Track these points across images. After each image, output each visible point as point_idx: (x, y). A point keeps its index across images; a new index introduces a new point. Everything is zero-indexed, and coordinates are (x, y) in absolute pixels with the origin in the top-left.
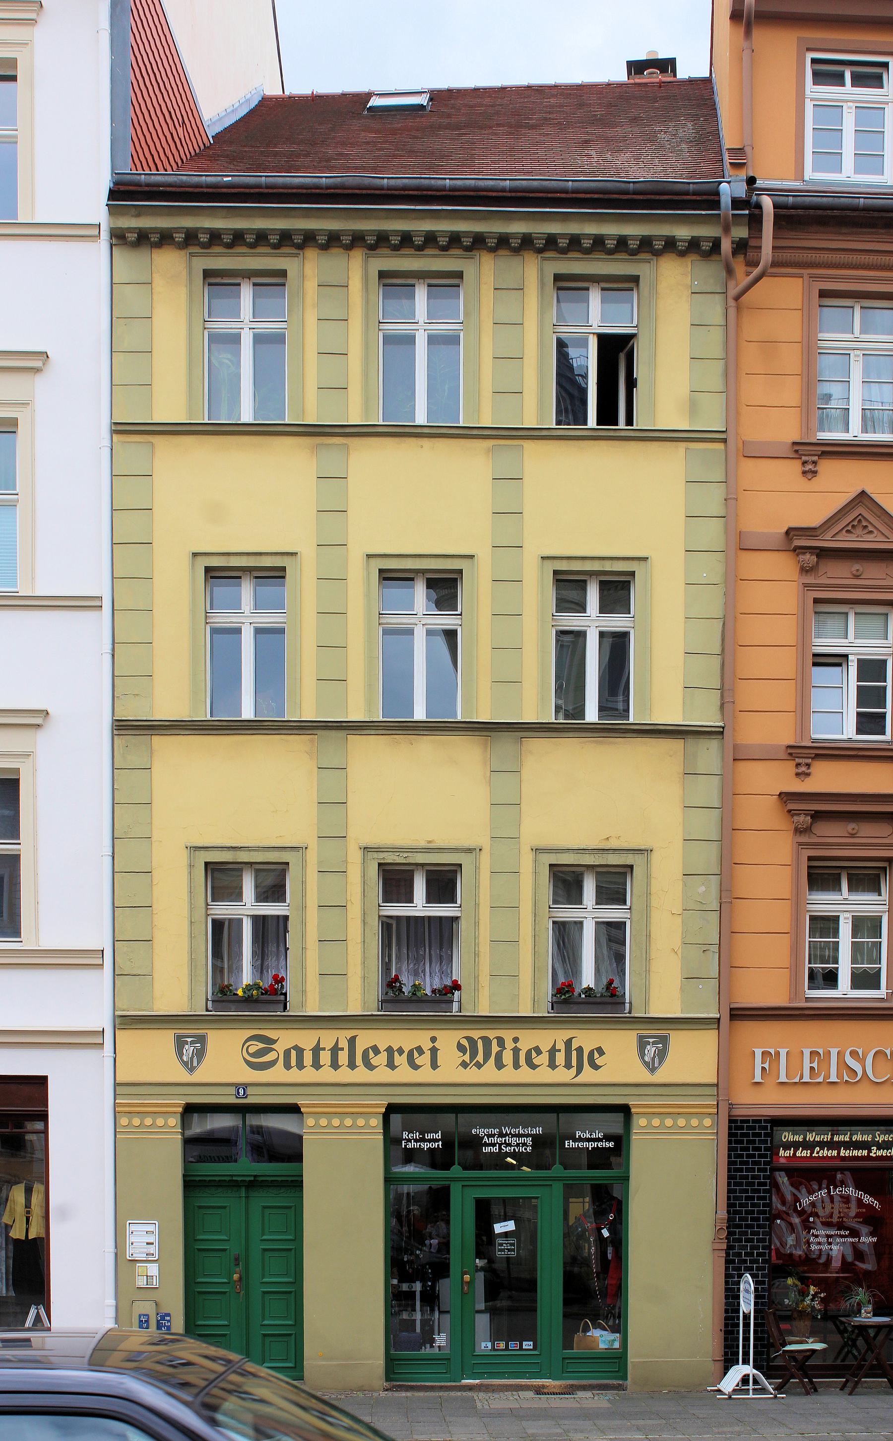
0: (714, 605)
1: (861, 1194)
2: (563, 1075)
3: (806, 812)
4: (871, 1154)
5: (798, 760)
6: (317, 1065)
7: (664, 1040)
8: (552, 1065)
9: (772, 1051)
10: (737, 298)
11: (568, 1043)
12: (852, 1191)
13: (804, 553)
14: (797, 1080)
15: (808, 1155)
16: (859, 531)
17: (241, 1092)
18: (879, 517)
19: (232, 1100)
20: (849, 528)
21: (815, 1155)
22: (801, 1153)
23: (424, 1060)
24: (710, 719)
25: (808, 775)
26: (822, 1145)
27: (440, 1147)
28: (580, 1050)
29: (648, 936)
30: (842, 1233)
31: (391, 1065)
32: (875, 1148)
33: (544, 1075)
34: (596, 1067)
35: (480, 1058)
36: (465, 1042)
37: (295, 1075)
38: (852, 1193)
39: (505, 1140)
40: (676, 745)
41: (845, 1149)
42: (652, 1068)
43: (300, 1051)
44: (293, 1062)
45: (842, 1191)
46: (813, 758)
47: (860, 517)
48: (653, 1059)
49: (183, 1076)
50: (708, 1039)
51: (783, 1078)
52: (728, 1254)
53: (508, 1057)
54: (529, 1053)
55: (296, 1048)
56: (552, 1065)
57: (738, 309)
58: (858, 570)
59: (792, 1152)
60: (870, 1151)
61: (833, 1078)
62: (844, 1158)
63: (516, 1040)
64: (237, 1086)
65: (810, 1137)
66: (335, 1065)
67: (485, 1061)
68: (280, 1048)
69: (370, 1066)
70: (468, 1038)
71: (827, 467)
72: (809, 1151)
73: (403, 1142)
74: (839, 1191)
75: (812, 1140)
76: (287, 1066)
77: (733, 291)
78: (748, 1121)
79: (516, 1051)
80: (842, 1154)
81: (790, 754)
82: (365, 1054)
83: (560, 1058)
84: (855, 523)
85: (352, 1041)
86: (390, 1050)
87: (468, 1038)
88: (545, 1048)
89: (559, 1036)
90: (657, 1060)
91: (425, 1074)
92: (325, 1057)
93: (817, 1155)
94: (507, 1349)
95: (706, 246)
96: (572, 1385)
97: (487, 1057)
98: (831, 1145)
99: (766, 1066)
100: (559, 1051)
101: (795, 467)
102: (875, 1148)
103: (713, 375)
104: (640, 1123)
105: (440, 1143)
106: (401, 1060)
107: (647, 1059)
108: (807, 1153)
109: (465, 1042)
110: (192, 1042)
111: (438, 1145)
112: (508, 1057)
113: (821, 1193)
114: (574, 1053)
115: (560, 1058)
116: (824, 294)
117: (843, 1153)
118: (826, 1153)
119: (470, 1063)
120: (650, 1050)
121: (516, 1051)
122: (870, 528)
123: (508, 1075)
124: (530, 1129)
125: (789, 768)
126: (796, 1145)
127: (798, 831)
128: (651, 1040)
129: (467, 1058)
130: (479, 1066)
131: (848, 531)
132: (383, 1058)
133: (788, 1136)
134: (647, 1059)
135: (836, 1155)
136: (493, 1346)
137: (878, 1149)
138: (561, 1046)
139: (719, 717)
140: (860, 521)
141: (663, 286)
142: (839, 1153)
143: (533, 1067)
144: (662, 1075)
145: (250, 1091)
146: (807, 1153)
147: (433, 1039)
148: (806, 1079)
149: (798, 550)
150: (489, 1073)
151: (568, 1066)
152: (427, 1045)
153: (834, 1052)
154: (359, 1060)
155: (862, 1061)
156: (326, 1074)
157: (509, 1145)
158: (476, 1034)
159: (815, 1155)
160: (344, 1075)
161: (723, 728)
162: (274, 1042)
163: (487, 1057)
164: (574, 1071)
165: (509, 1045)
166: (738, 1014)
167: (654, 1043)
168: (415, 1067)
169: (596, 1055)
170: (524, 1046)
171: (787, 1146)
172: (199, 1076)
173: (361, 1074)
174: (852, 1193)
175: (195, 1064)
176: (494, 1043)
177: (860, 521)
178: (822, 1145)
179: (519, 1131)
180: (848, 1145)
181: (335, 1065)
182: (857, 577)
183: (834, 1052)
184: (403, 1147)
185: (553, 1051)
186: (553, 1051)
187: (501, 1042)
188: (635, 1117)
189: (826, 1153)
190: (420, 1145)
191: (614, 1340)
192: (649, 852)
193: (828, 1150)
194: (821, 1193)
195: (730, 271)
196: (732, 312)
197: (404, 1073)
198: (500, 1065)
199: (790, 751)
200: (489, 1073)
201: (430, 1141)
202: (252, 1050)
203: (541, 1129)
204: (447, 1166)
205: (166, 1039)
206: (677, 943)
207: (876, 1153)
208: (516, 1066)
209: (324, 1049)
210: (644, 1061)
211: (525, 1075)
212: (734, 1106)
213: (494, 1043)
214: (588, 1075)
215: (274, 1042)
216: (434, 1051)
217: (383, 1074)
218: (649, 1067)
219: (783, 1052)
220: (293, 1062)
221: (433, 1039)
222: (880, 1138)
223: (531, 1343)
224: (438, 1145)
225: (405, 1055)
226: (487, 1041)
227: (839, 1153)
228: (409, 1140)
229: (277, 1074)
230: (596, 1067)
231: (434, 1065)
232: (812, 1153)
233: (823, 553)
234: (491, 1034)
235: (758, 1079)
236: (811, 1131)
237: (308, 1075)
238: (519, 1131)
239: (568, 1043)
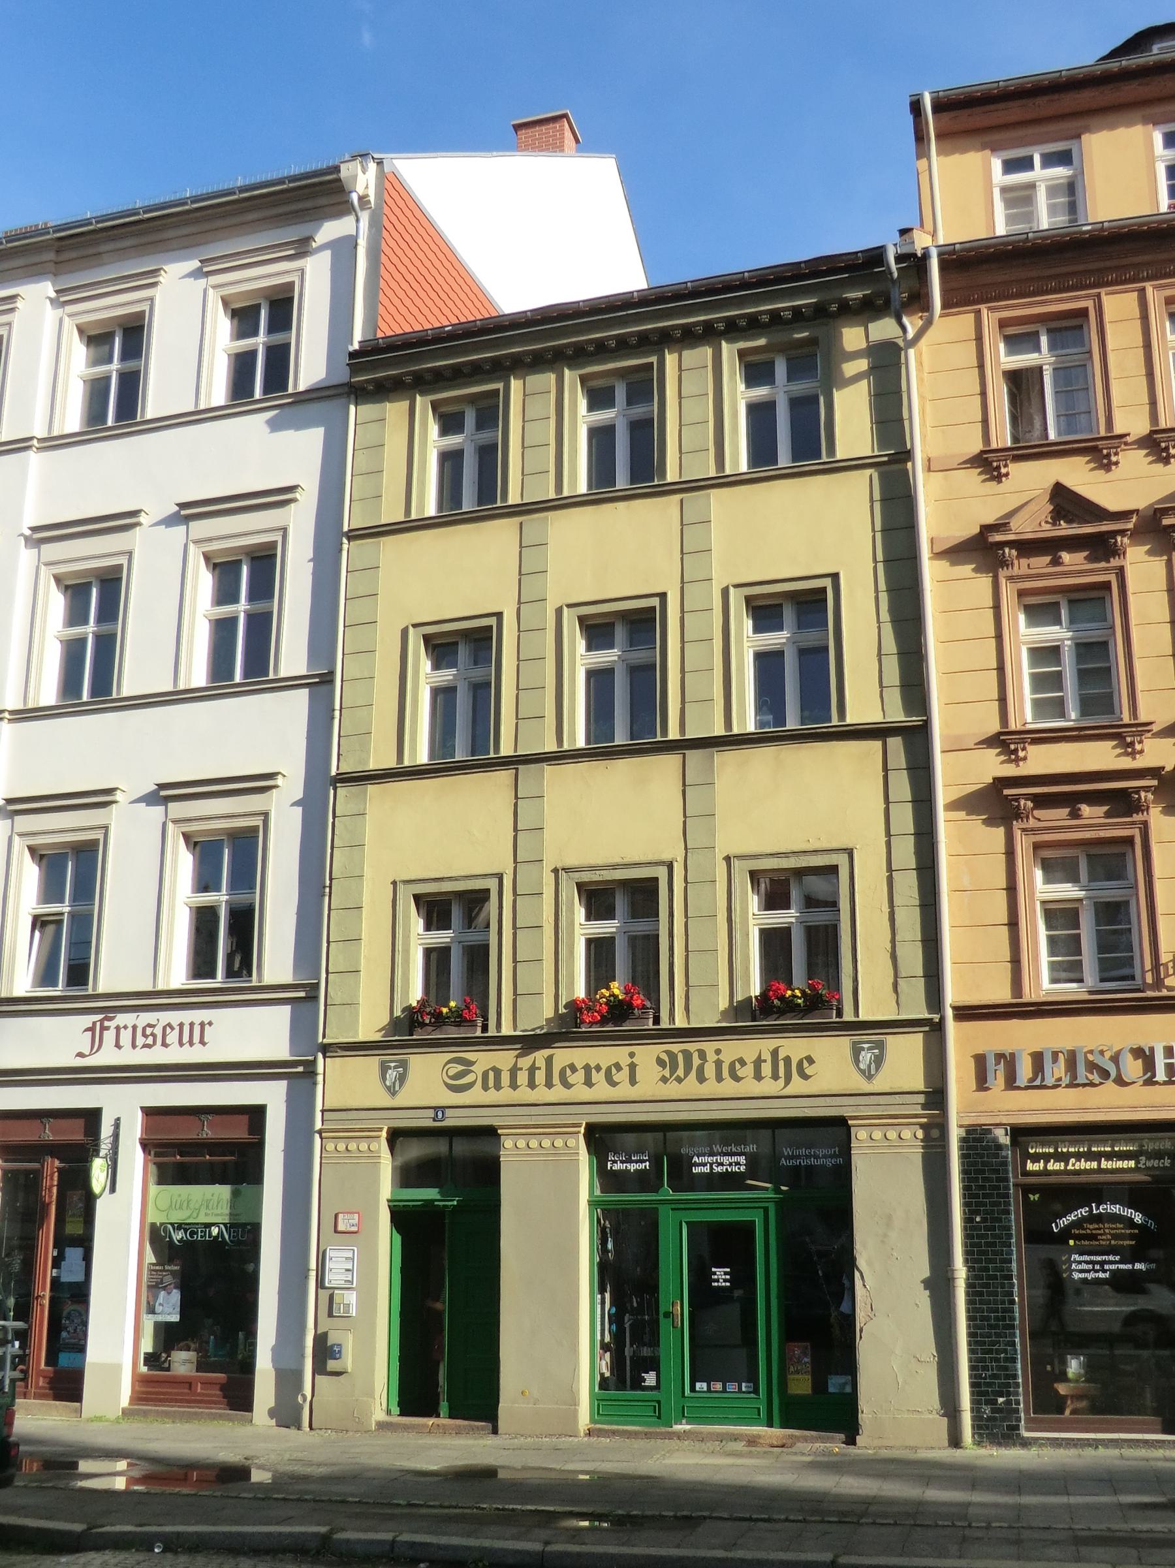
1: (1131, 1213)
2: (769, 1086)
4: (1139, 1166)
6: (514, 1085)
7: (880, 1045)
8: (758, 1077)
11: (775, 1053)
12: (1120, 1209)
15: (1062, 1168)
17: (440, 1115)
19: (429, 1123)
22: (1053, 1166)
23: (622, 1076)
27: (648, 1168)
28: (788, 1060)
31: (588, 1083)
33: (750, 1087)
34: (806, 1077)
35: (680, 1072)
36: (665, 1057)
37: (492, 1096)
38: (1120, 1210)
39: (717, 1160)
41: (1107, 1160)
42: (870, 1077)
43: (497, 1072)
44: (491, 1083)
45: (1107, 1209)
48: (869, 1067)
49: (386, 1101)
53: (710, 1070)
54: (732, 1065)
55: (494, 1069)
56: (758, 1077)
62: (1107, 1171)
63: (718, 1052)
64: (436, 1109)
66: (532, 1085)
67: (686, 1075)
68: (478, 1069)
69: (567, 1085)
70: (667, 1052)
72: (1063, 1164)
73: (609, 1163)
74: (1103, 1209)
76: (485, 1087)
79: (719, 1064)
80: (1103, 1166)
82: (562, 1073)
83: (766, 1069)
85: (549, 1061)
86: (587, 1068)
87: (667, 1052)
88: (750, 1058)
89: (763, 1046)
90: (873, 1066)
91: (624, 1091)
92: (522, 1078)
93: (1073, 1168)
94: (724, 1391)
96: (792, 1435)
97: (687, 1072)
98: (1090, 1156)
100: (765, 1061)
104: (860, 1135)
105: (648, 1163)
106: (598, 1077)
107: (862, 1066)
109: (665, 1057)
110: (395, 1067)
111: (645, 1166)
112: (710, 1070)
113: (1081, 1212)
114: (781, 1064)
115: (766, 1069)
117: (1105, 1164)
118: (1083, 1165)
119: (671, 1077)
120: (866, 1057)
121: (719, 1064)
123: (711, 1088)
124: (743, 1146)
129: (667, 1073)
130: (679, 1080)
132: (580, 1076)
134: (862, 1066)
135: (1096, 1167)
136: (709, 1386)
137: (1149, 1158)
138: (767, 1056)
143: (737, 1079)
144: (878, 1085)
145: (448, 1112)
147: (632, 1055)
150: (691, 1087)
151: (775, 1077)
152: (625, 1061)
154: (556, 1079)
156: (524, 1094)
157: (722, 1164)
158: (675, 1048)
159: (1070, 1167)
160: (542, 1094)
162: (472, 1063)
163: (687, 1072)
164: (781, 1082)
165: (711, 1057)
167: (869, 1049)
168: (613, 1084)
169: (806, 1064)
170: (727, 1058)
171: (1036, 1158)
172: (401, 1100)
173: (559, 1093)
174: (1120, 1210)
175: (397, 1088)
176: (695, 1056)
178: (1078, 1156)
179: (731, 1150)
180: (1109, 1156)
181: (532, 1085)
184: (609, 1168)
185: (758, 1062)
186: (758, 1062)
187: (702, 1055)
188: (853, 1130)
189: (1083, 1165)
190: (626, 1167)
191: (845, 1384)
193: (1086, 1161)
194: (1081, 1212)
197: (602, 1091)
198: (701, 1078)
200: (691, 1087)
201: (636, 1162)
202: (452, 1073)
203: (755, 1146)
204: (656, 1189)
205: (371, 1064)
207: (1145, 1164)
208: (719, 1078)
209: (521, 1069)
210: (859, 1069)
211: (729, 1087)
213: (695, 1056)
214: (798, 1085)
215: (472, 1063)
216: (633, 1067)
217: (581, 1092)
218: (865, 1075)
220: (491, 1083)
221: (632, 1055)
223: (752, 1384)
224: (645, 1166)
225: (603, 1072)
226: (688, 1055)
227: (1099, 1164)
228: (615, 1162)
229: (476, 1095)
230: (806, 1077)
231: (633, 1081)
232: (1067, 1164)
234: (692, 1047)
237: (506, 1095)
238: (731, 1150)
239: (775, 1053)
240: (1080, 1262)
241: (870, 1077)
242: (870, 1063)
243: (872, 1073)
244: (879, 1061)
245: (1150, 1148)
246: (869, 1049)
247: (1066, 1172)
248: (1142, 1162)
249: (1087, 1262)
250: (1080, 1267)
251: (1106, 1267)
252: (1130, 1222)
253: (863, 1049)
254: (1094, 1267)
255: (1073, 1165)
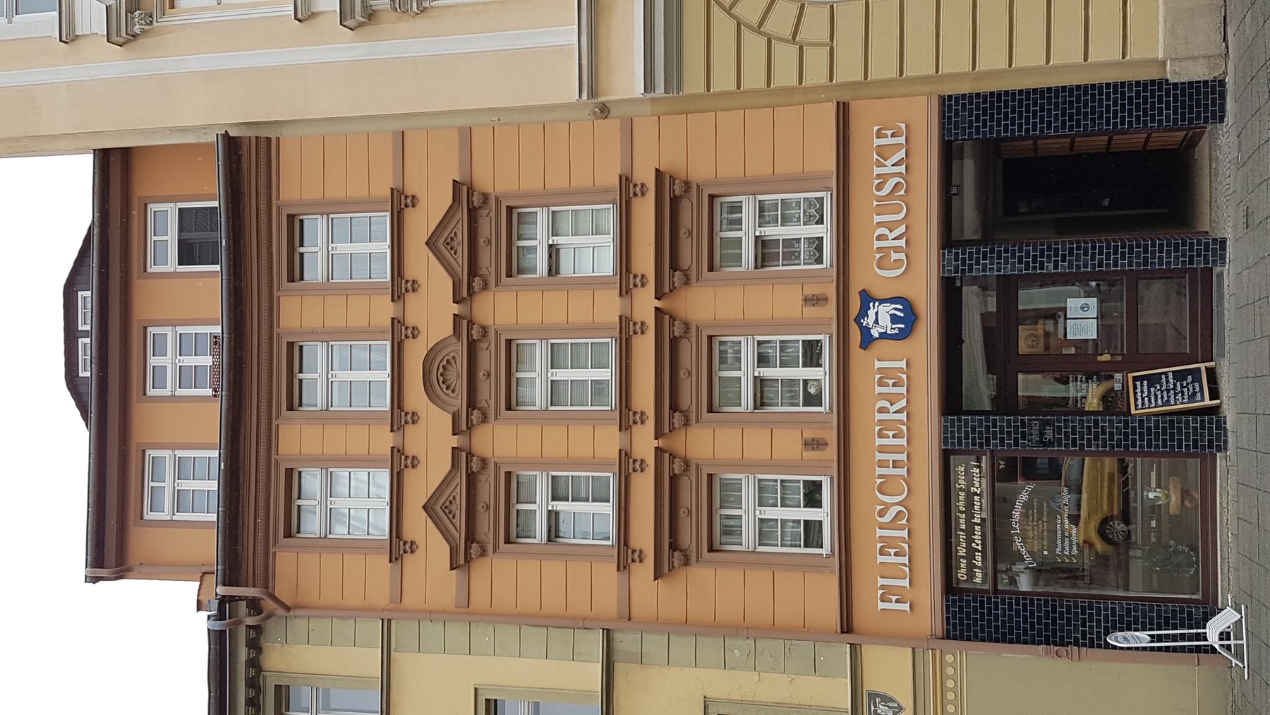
0: (508, 633)
1: (1019, 502)
3: (671, 556)
5: (629, 561)
7: (872, 696)
9: (880, 592)
10: (288, 609)
13: (470, 554)
14: (907, 569)
15: (980, 554)
16: (453, 507)
18: (442, 492)
20: (451, 516)
21: (979, 548)
24: (597, 639)
25: (641, 551)
26: (970, 540)
29: (778, 704)
30: (1059, 522)
32: (972, 488)
38: (1017, 512)
40: (619, 669)
42: (900, 708)
45: (1016, 522)
46: (628, 548)
47: (443, 507)
50: (873, 655)
51: (906, 583)
52: (1084, 645)
57: (299, 607)
58: (483, 507)
59: (977, 570)
60: (976, 494)
61: (905, 534)
65: (962, 552)
71: (409, 532)
72: (976, 553)
74: (1016, 525)
75: (965, 551)
77: (280, 612)
78: (948, 618)
80: (979, 521)
81: (624, 568)
84: (447, 511)
93: (980, 546)
95: (253, 634)
99: (894, 598)
101: (408, 558)
102: (972, 488)
103: (344, 628)
108: (978, 556)
113: (1019, 542)
116: (288, 534)
122: (451, 498)
125: (635, 567)
126: (971, 567)
127: (686, 562)
128: (873, 708)
131: (454, 517)
133: (962, 574)
139: (596, 632)
140: (446, 507)
141: (283, 667)
142: (978, 524)
146: (978, 556)
148: (905, 560)
149: (468, 559)
153: (879, 533)
155: (888, 506)
159: (979, 548)
161: (604, 629)
166: (847, 626)
171: (971, 575)
174: (1017, 512)
177: (446, 507)
178: (970, 540)
182: (488, 507)
183: (879, 533)
192: (706, 699)
193: (975, 535)
194: (1019, 542)
195: (269, 616)
196: (298, 612)
199: (622, 568)
206: (784, 678)
212: (934, 633)
219: (881, 582)
222: (962, 483)
227: (978, 524)
232: (979, 551)
233: (471, 538)
235: (906, 607)
236: (957, 551)
240: (1063, 548)
241: (900, 708)
242: (888, 706)
243: (896, 705)
244: (886, 699)
245: (963, 482)
246: (875, 706)
247: (984, 552)
248: (975, 490)
249: (1063, 542)
250: (1067, 548)
251: (1067, 527)
252: (1027, 506)
253: (875, 711)
254: (1067, 537)
255: (978, 545)
